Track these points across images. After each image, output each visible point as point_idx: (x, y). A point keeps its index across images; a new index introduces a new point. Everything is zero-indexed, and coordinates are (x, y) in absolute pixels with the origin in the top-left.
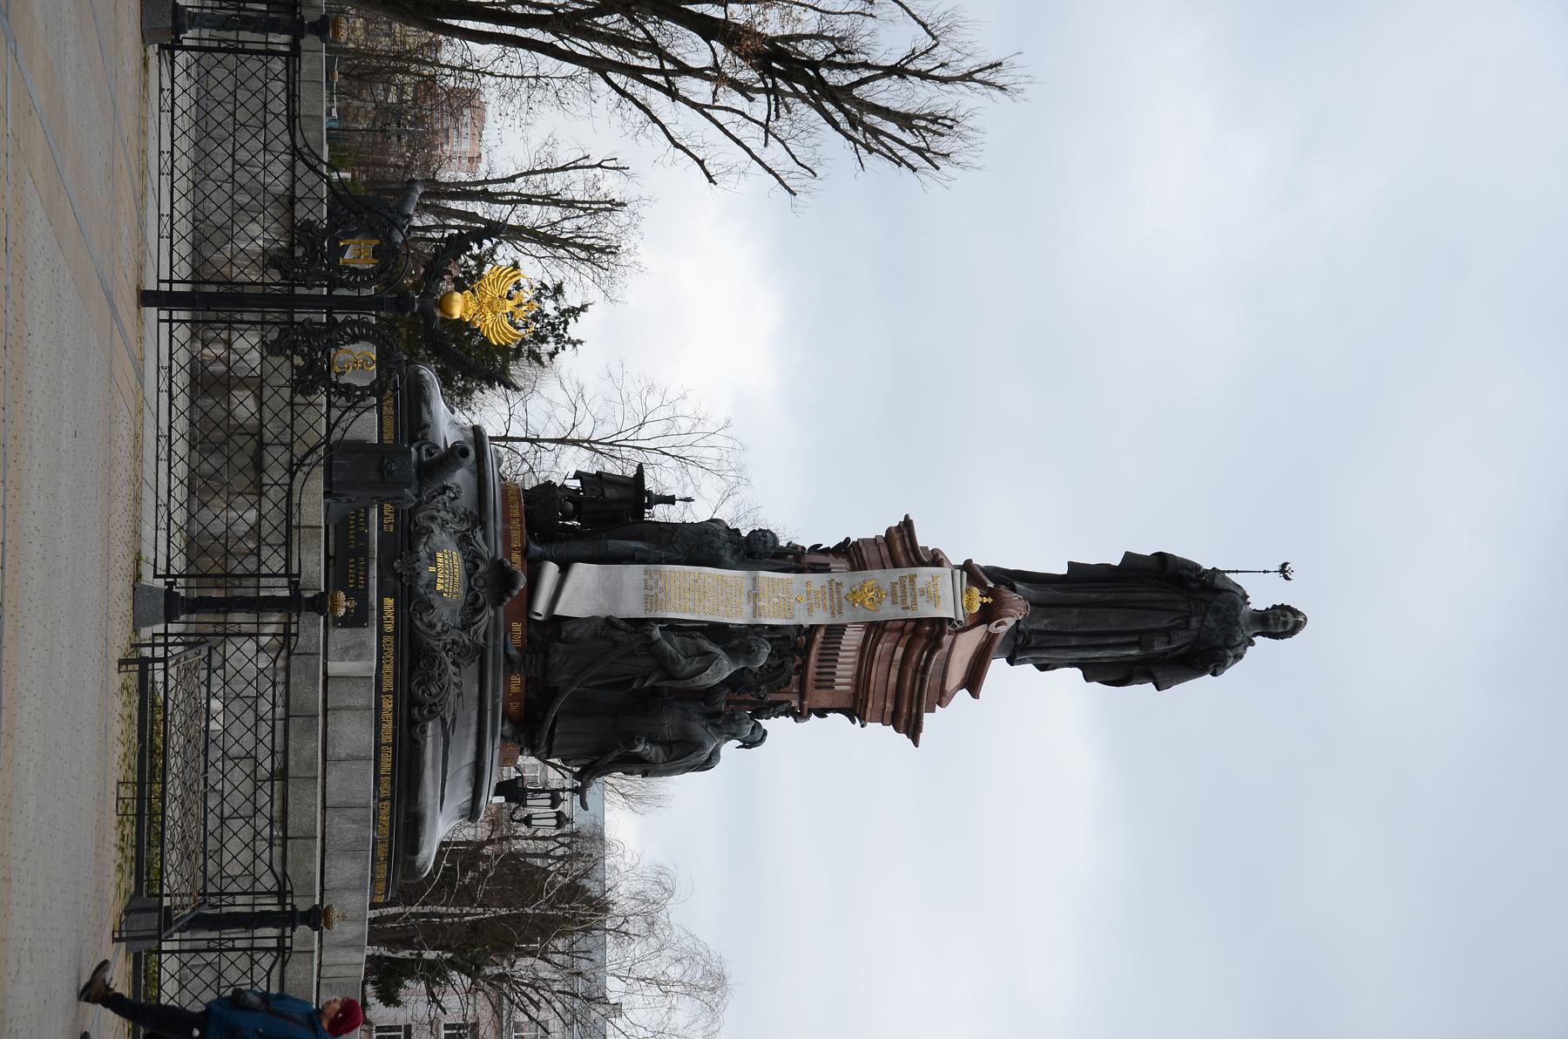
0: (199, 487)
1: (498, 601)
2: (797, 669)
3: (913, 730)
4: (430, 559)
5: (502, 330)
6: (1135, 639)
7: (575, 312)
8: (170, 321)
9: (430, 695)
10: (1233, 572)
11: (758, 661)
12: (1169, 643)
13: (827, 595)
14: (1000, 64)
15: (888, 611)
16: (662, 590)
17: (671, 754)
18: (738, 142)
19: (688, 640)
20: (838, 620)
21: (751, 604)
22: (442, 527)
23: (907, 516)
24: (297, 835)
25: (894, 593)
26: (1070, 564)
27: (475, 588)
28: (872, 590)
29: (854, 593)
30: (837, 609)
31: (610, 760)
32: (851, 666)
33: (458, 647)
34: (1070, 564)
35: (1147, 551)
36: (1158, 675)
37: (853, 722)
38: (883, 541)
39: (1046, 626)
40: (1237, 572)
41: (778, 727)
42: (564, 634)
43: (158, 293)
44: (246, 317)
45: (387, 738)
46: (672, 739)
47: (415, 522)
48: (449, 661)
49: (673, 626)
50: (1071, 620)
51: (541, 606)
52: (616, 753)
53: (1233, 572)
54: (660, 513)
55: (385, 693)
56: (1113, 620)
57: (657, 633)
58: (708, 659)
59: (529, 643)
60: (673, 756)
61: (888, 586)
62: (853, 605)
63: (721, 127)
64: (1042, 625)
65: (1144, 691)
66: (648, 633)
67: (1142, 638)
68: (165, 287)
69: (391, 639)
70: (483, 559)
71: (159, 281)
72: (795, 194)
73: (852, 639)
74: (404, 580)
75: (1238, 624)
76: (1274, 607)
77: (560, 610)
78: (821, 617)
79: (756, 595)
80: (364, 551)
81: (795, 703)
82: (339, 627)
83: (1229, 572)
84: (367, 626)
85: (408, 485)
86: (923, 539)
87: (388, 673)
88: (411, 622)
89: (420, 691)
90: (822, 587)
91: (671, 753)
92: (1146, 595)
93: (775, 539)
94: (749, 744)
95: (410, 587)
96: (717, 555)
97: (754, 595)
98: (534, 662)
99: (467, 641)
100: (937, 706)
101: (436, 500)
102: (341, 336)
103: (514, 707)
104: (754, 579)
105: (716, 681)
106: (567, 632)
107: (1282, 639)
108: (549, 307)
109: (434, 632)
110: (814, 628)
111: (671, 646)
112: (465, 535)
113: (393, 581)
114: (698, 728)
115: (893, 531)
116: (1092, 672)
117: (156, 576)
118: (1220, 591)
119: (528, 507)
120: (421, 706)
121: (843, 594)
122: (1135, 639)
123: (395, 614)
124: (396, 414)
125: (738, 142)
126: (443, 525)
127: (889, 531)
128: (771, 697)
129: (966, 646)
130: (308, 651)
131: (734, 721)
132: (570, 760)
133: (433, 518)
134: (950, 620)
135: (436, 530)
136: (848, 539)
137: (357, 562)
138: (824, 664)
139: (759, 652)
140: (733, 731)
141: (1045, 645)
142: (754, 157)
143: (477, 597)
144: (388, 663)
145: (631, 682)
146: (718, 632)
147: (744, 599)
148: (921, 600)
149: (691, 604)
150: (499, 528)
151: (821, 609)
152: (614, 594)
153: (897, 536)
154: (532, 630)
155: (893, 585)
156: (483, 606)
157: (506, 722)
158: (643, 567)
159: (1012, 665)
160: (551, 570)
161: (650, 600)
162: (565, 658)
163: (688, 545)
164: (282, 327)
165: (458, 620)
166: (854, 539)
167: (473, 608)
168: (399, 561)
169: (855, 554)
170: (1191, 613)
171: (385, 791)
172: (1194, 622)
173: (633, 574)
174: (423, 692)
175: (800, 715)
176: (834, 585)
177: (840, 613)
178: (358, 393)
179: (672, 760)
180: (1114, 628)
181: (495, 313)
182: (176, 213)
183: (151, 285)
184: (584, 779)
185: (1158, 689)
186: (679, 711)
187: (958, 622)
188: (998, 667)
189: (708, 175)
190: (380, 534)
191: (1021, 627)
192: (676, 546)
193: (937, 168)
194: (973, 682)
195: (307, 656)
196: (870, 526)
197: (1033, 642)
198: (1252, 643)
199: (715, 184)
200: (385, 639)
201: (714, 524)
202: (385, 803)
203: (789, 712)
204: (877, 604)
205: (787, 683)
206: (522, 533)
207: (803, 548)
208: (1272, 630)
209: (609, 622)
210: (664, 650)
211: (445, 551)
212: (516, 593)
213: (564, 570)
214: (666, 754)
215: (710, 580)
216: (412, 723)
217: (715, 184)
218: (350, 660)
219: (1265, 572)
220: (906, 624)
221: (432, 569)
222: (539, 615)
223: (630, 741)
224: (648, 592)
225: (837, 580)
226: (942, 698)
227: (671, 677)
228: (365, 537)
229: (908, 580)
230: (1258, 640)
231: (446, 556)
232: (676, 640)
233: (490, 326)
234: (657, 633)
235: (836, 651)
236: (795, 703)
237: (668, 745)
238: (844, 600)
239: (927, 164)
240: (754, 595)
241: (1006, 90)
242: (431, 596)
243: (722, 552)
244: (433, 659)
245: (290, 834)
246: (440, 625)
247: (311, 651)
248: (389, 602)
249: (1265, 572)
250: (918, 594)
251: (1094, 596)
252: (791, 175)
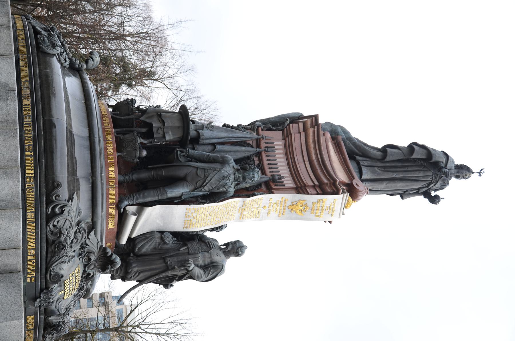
28: (302, 206)
90: (277, 201)
98: (119, 272)
124: (36, 185)
147: (237, 211)
151: (277, 215)
162: (137, 274)
163: (212, 187)
173: (180, 210)
176: (284, 200)
190: (25, 284)
206: (116, 192)
225: (286, 198)
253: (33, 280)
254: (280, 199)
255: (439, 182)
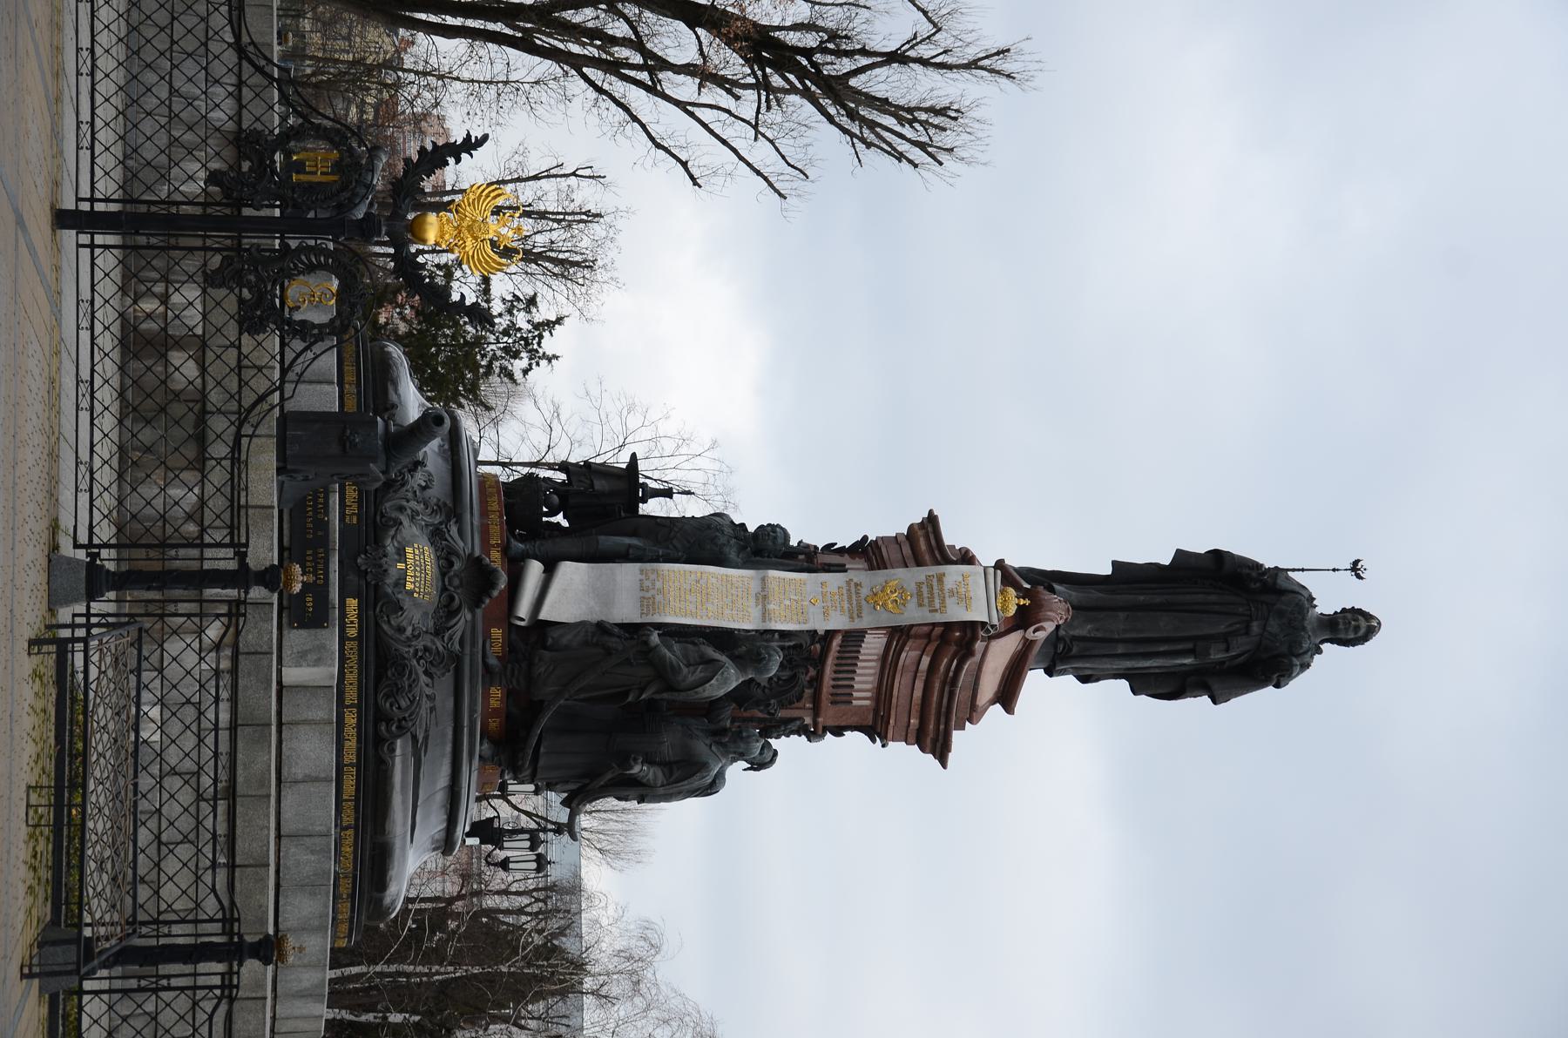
0: (129, 463)
1: (476, 603)
2: (811, 682)
3: (941, 751)
4: (399, 554)
5: (484, 258)
6: (1189, 646)
7: (549, 325)
8: (92, 246)
9: (399, 708)
10: (1299, 570)
11: (768, 671)
12: (1227, 650)
13: (845, 597)
14: (1008, 50)
15: (914, 614)
16: (660, 591)
17: (670, 777)
18: (724, 142)
19: (690, 647)
20: (858, 625)
21: (760, 607)
22: (412, 518)
23: (931, 512)
24: (246, 863)
25: (920, 595)
26: (1115, 563)
27: (449, 588)
29: (875, 595)
30: (856, 613)
31: (602, 783)
32: (871, 679)
33: (430, 654)
34: (1115, 563)
35: (1201, 549)
36: (1215, 686)
37: (874, 741)
38: (904, 539)
39: (1089, 632)
40: (1303, 570)
41: (788, 746)
42: (550, 641)
43: (77, 213)
44: (184, 242)
45: (350, 757)
46: (672, 759)
47: (382, 513)
48: (420, 670)
51: (524, 609)
52: (609, 776)
53: (1299, 570)
54: (653, 507)
55: (348, 707)
56: (1165, 625)
57: (655, 638)
58: (713, 667)
59: (510, 652)
60: (674, 777)
61: (913, 586)
62: (875, 608)
63: (705, 126)
64: (1083, 631)
65: (1199, 704)
66: (644, 638)
67: (1196, 645)
68: (85, 206)
69: (354, 644)
70: (458, 556)
71: (78, 199)
72: (785, 198)
73: (873, 645)
74: (369, 578)
75: (1304, 629)
76: (1344, 610)
77: (544, 615)
78: (838, 622)
79: (765, 597)
80: (324, 542)
81: (808, 720)
82: (294, 628)
83: (1294, 570)
84: (327, 627)
85: (374, 459)
86: (952, 536)
87: (351, 684)
88: (377, 625)
89: (388, 705)
91: (671, 774)
92: (1200, 597)
93: (786, 536)
94: (758, 765)
95: (377, 587)
96: (721, 553)
97: (763, 598)
98: (516, 672)
99: (441, 648)
100: (967, 723)
101: (405, 488)
102: (295, 265)
103: (494, 724)
104: (763, 580)
105: (722, 693)
106: (553, 638)
107: (1353, 646)
108: (521, 320)
109: (403, 637)
110: (830, 634)
111: (671, 653)
112: (438, 529)
113: (357, 579)
114: (701, 747)
115: (916, 527)
116: (1141, 684)
117: (76, 546)
118: (1282, 592)
119: (510, 501)
120: (389, 721)
121: (863, 596)
122: (1189, 646)
123: (359, 616)
124: (359, 393)
125: (724, 142)
126: (413, 517)
127: (911, 528)
128: (782, 714)
129: (1000, 653)
130: (259, 650)
131: (742, 738)
132: (556, 784)
133: (401, 509)
134: (983, 624)
135: (406, 522)
136: (865, 538)
137: (315, 554)
138: (841, 676)
139: (769, 660)
140: (741, 750)
141: (1088, 653)
142: (741, 158)
143: (452, 599)
144: (351, 672)
145: (626, 694)
146: (723, 638)
147: (752, 601)
148: (950, 602)
149: (691, 607)
150: (476, 522)
151: (838, 613)
152: (606, 597)
153: (920, 533)
154: (514, 636)
155: (919, 585)
156: (458, 610)
157: (486, 741)
158: (638, 565)
159: (1051, 676)
160: (535, 569)
161: (647, 603)
162: (551, 668)
163: (689, 542)
164: (225, 253)
165: (431, 624)
166: (872, 537)
167: (447, 610)
168: (363, 556)
169: (874, 554)
170: (1251, 616)
171: (349, 818)
172: (1255, 627)
173: (627, 573)
174: (391, 706)
175: (813, 734)
177: (859, 616)
178: (316, 331)
179: (673, 783)
180: (1165, 635)
181: (476, 238)
182: (97, 121)
183: (69, 204)
184: (574, 805)
185: (1215, 702)
186: (680, 728)
187: (993, 626)
188: (1035, 680)
189: (692, 177)
191: (1062, 633)
192: (675, 542)
193: (941, 164)
194: (1007, 696)
195: (258, 656)
196: (890, 523)
197: (1075, 650)
198: (1319, 651)
199: (700, 187)
200: (348, 645)
201: (717, 519)
202: (348, 832)
203: (802, 730)
204: (902, 607)
205: (799, 699)
206: (502, 528)
207: (816, 547)
208: (1342, 636)
209: (601, 627)
210: (662, 658)
211: (416, 546)
212: (495, 593)
213: (550, 571)
214: (664, 774)
215: (714, 580)
216: (379, 741)
217: (700, 187)
218: (308, 666)
219: (1334, 570)
220: (933, 629)
221: (401, 566)
222: (522, 620)
223: (625, 760)
224: (642, 594)
225: (855, 580)
226: (973, 714)
227: (671, 688)
228: (324, 526)
229: (935, 580)
230: (1326, 647)
231: (417, 552)
232: (676, 647)
233: (471, 254)
234: (655, 638)
235: (854, 662)
236: (808, 720)
237: (667, 766)
238: (864, 603)
239: (930, 160)
240: (763, 598)
241: (1014, 78)
242: (400, 596)
243: (727, 550)
244: (401, 666)
245: (238, 861)
246: (409, 629)
247: (263, 650)
248: (352, 603)
249: (1334, 570)
250: (947, 595)
251: (1142, 598)
252: (781, 178)
253: (355, 520)
254: (844, 585)
255: (1271, 619)
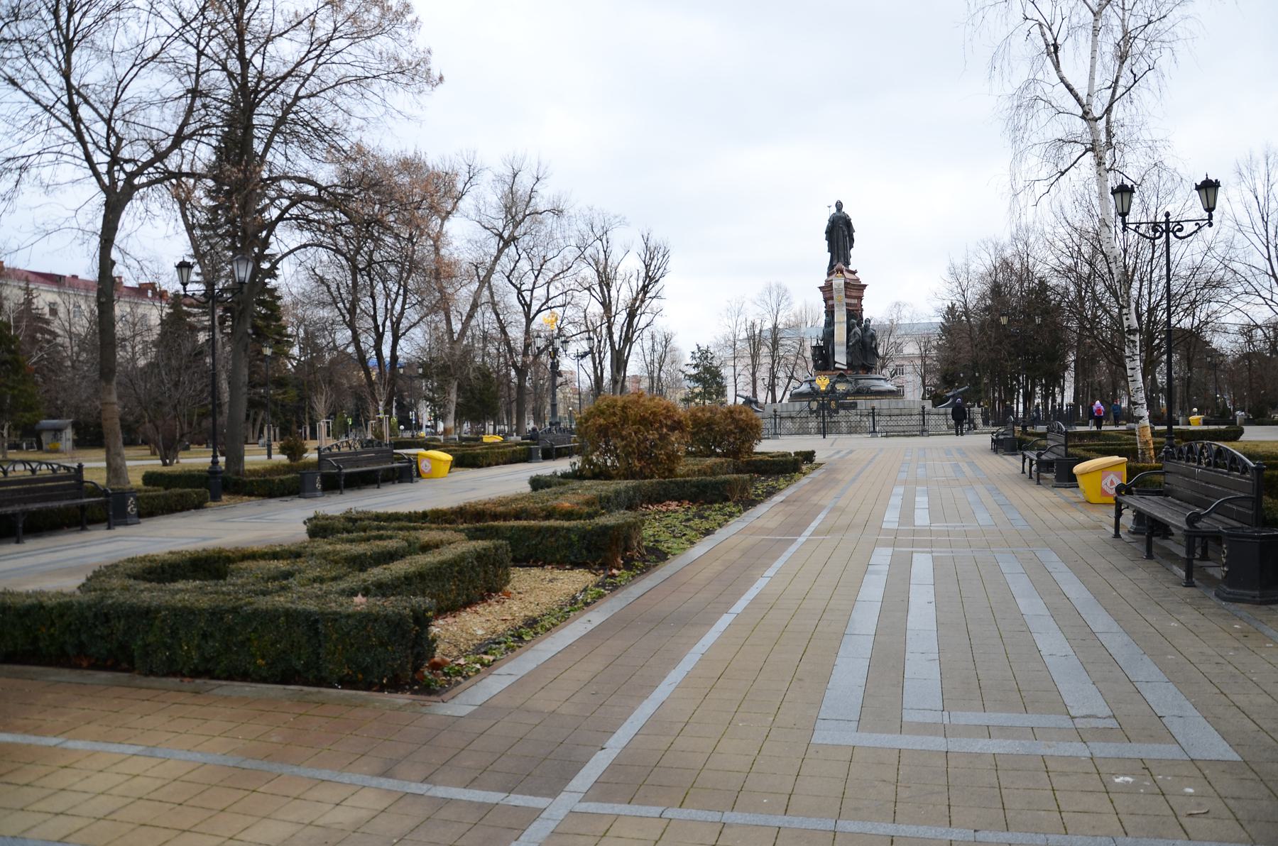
0: (840, 433)
3: (865, 286)
7: (699, 348)
15: (843, 294)
49: (848, 341)
50: (841, 252)
56: (841, 243)
58: (855, 333)
65: (855, 235)
67: (844, 237)
78: (844, 308)
108: (697, 355)
114: (869, 334)
116: (851, 247)
129: (848, 275)
146: (849, 330)
160: (837, 365)
161: (842, 344)
167: (847, 381)
188: (851, 268)
194: (854, 273)
209: (847, 353)
213: (835, 363)
223: (871, 348)
226: (858, 280)
244: (858, 389)
